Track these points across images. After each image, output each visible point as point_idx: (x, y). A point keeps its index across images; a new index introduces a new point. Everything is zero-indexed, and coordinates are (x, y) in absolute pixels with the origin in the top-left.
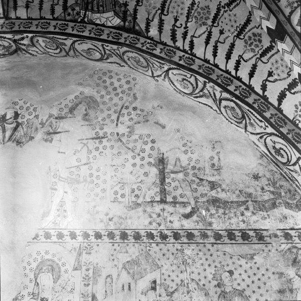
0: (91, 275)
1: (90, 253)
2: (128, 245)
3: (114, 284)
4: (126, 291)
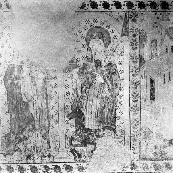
0: (138, 40)
1: (136, 21)
2: (169, 14)
3: (158, 48)
4: (169, 53)
